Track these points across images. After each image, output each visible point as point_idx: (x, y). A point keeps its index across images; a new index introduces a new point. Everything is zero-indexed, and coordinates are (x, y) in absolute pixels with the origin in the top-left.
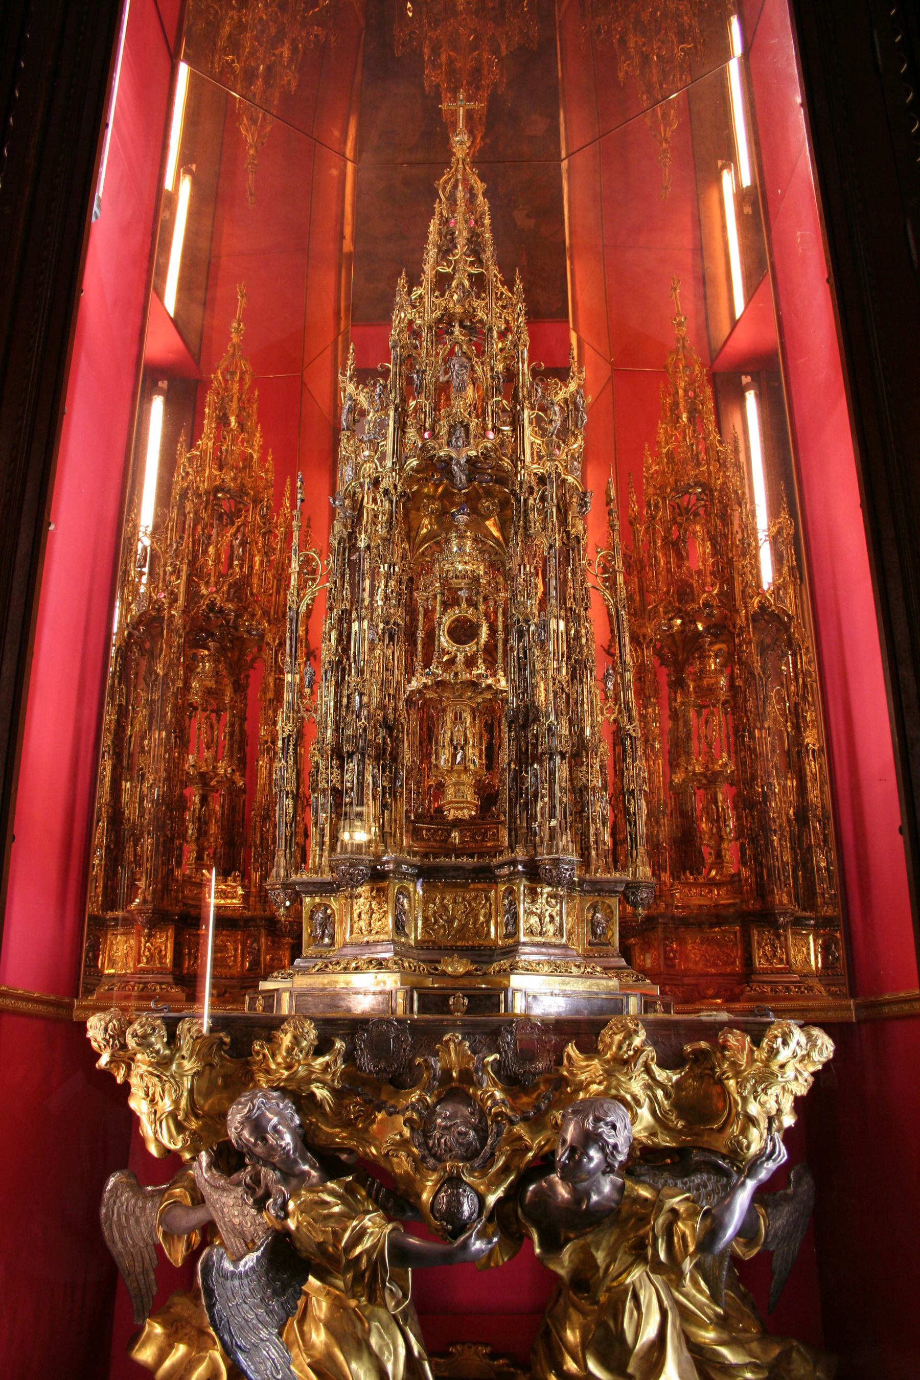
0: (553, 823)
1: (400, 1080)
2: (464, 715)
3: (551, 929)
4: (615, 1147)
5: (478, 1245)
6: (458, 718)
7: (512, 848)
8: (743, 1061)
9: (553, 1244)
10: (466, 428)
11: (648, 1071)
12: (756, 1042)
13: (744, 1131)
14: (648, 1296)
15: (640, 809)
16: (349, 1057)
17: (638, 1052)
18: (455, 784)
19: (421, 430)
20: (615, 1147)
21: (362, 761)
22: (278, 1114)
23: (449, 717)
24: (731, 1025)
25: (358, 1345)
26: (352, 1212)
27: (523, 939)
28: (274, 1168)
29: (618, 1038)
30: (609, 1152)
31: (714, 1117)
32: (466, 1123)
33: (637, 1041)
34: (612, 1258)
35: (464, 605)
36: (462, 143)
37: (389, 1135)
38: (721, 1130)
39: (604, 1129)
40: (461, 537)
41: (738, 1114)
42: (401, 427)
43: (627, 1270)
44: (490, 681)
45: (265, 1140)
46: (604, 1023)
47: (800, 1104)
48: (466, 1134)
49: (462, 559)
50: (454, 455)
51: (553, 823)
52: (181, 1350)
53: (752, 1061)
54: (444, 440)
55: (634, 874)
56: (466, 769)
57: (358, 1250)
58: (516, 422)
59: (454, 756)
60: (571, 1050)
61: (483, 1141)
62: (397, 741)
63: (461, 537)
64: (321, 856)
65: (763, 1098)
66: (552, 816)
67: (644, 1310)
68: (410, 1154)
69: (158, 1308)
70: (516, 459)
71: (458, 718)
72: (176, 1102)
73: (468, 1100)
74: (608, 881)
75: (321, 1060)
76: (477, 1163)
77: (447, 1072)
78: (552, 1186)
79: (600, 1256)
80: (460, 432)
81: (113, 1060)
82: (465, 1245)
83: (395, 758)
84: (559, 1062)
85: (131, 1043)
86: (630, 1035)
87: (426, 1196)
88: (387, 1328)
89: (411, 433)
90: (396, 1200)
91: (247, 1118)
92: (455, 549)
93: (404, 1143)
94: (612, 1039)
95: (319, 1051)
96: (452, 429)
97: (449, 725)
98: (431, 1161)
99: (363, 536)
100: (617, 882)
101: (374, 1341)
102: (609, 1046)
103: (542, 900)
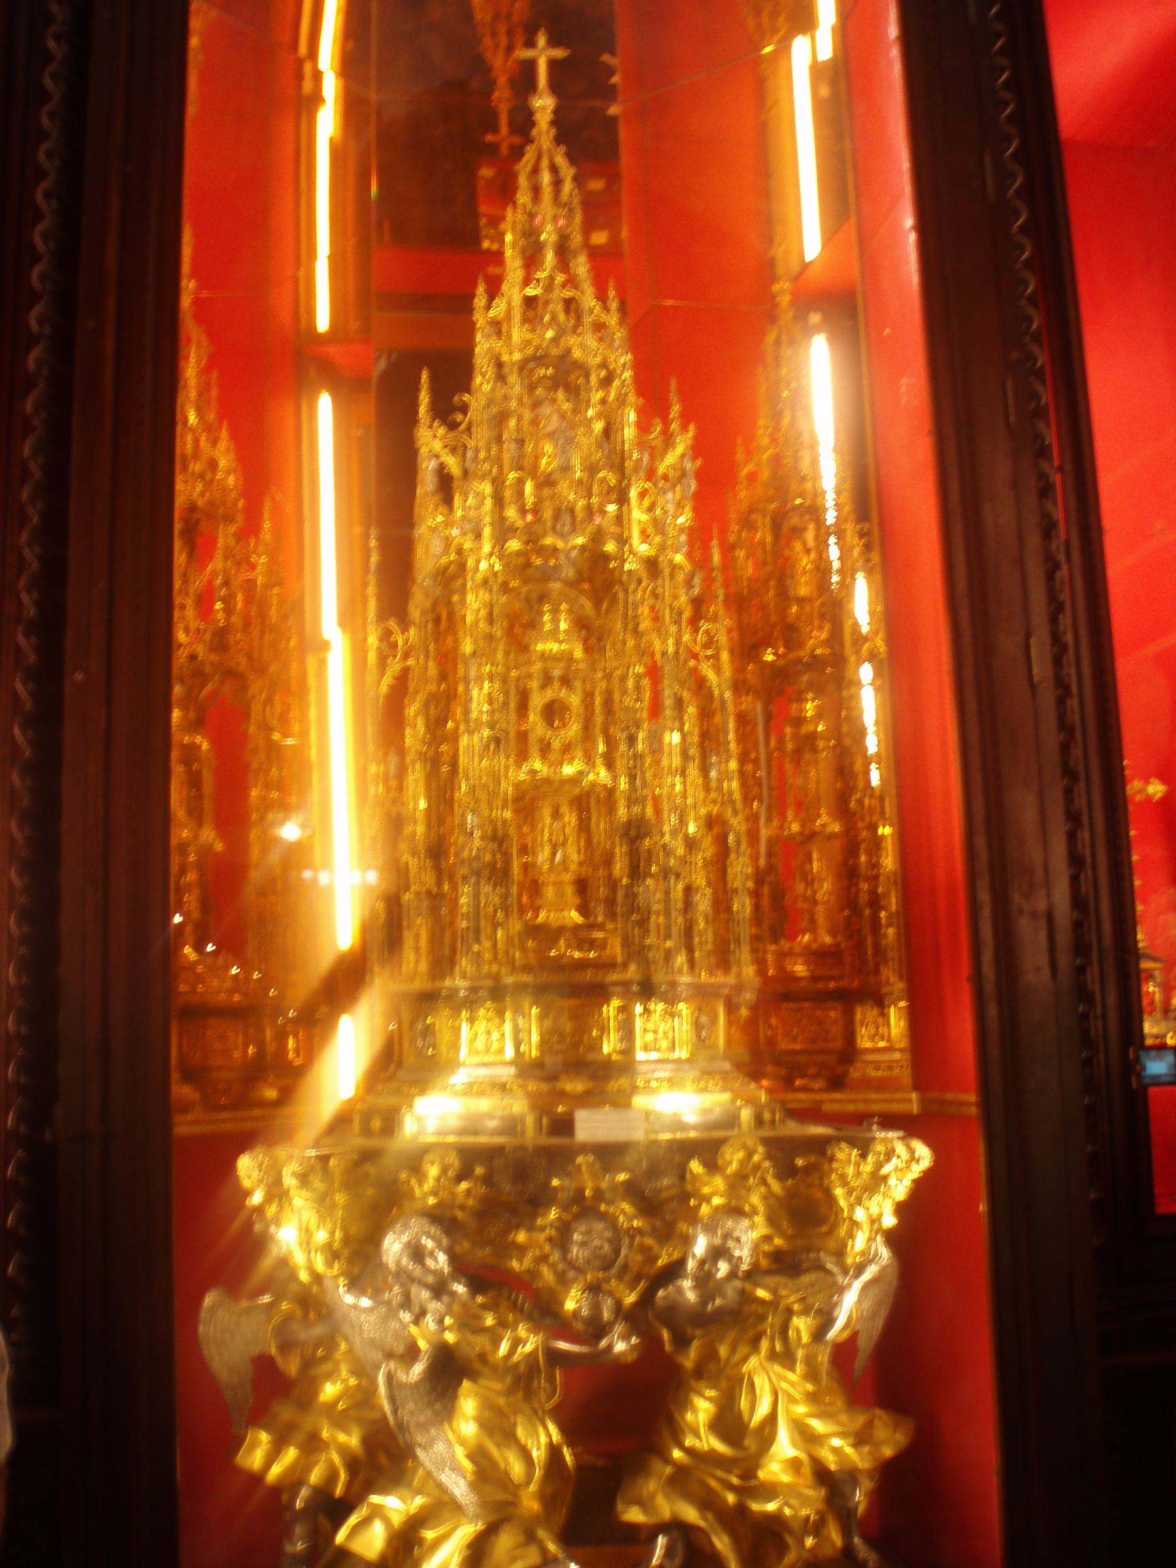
0: (669, 944)
1: (537, 1202)
2: (561, 810)
3: (664, 1044)
4: (740, 1258)
5: (620, 1347)
6: (556, 814)
7: (625, 966)
8: (851, 1170)
9: (682, 1341)
10: (572, 511)
11: (764, 1182)
12: (864, 1156)
13: (851, 1235)
14: (762, 1383)
15: (743, 906)
16: (488, 1180)
17: (757, 1167)
18: (555, 884)
19: (523, 512)
20: (740, 1258)
21: (478, 883)
22: (433, 1238)
23: (546, 813)
24: (839, 1139)
25: (509, 1437)
26: (502, 1324)
27: (640, 1056)
28: (427, 1286)
29: (741, 1155)
30: (735, 1263)
31: (821, 1221)
32: (601, 1238)
33: (756, 1158)
34: (733, 1350)
35: (556, 685)
36: (544, 108)
37: (530, 1247)
38: (830, 1233)
39: (731, 1244)
40: (555, 611)
41: (844, 1220)
42: (499, 501)
43: (745, 1359)
44: (591, 777)
45: (423, 1265)
46: (723, 1141)
47: (901, 1209)
48: (601, 1247)
49: (556, 638)
50: (560, 544)
51: (669, 944)
52: (291, 1454)
53: (858, 1174)
54: (549, 524)
55: (739, 975)
56: (566, 869)
57: (516, 1358)
58: (622, 499)
59: (554, 854)
60: (695, 1166)
61: (617, 1252)
62: (507, 856)
63: (555, 611)
64: (417, 962)
65: (867, 1203)
66: (668, 936)
67: (758, 1392)
68: (553, 1267)
69: (258, 1416)
70: (623, 541)
71: (556, 814)
72: (332, 1233)
73: (603, 1217)
74: (712, 985)
75: (464, 1185)
76: (614, 1270)
77: (580, 1192)
78: (680, 1291)
79: (723, 1351)
80: (567, 518)
81: (268, 1199)
82: (610, 1347)
83: (506, 873)
84: (682, 1177)
85: (289, 1181)
86: (750, 1155)
87: (570, 1305)
88: (530, 1420)
89: (511, 513)
90: (545, 1312)
91: (408, 1245)
92: (548, 627)
93: (544, 1258)
94: (733, 1158)
95: (459, 1178)
96: (557, 516)
97: (548, 821)
98: (571, 1274)
99: (468, 638)
100: (721, 986)
101: (520, 1432)
102: (730, 1163)
103: (656, 1017)
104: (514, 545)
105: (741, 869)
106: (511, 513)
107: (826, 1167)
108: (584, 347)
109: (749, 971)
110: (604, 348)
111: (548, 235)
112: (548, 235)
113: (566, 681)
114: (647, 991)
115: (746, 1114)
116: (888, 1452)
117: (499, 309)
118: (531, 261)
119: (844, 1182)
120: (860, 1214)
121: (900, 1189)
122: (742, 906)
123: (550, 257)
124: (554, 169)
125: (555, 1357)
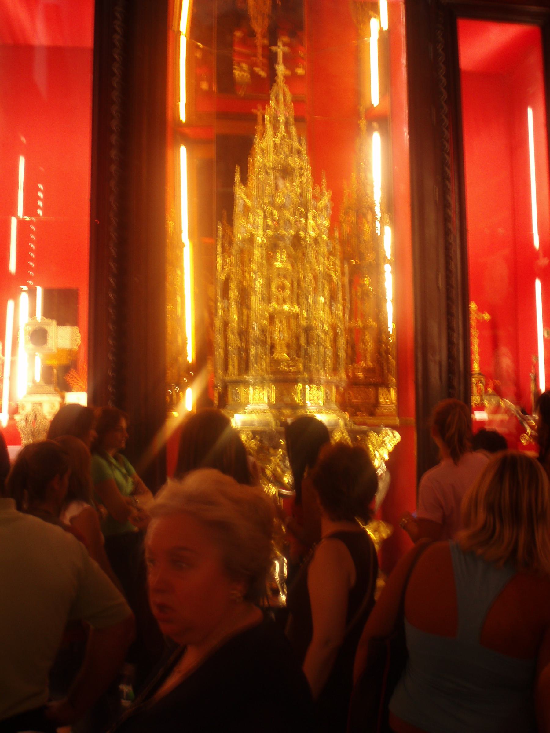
16: (261, 441)
42: (265, 217)
47: (390, 454)
58: (306, 217)
70: (306, 231)
104: (270, 232)
105: (342, 341)
106: (269, 221)
107: (366, 438)
108: (294, 162)
109: (343, 376)
110: (301, 163)
111: (282, 119)
112: (282, 119)
113: (285, 277)
114: (311, 382)
115: (342, 423)
116: (384, 535)
117: (264, 145)
118: (276, 128)
119: (372, 443)
120: (377, 453)
121: (390, 447)
122: (342, 354)
123: (282, 127)
124: (284, 95)
125: (281, 495)
